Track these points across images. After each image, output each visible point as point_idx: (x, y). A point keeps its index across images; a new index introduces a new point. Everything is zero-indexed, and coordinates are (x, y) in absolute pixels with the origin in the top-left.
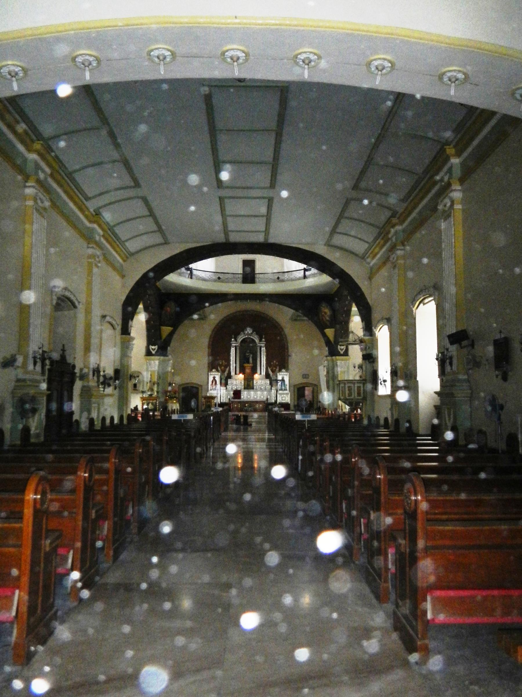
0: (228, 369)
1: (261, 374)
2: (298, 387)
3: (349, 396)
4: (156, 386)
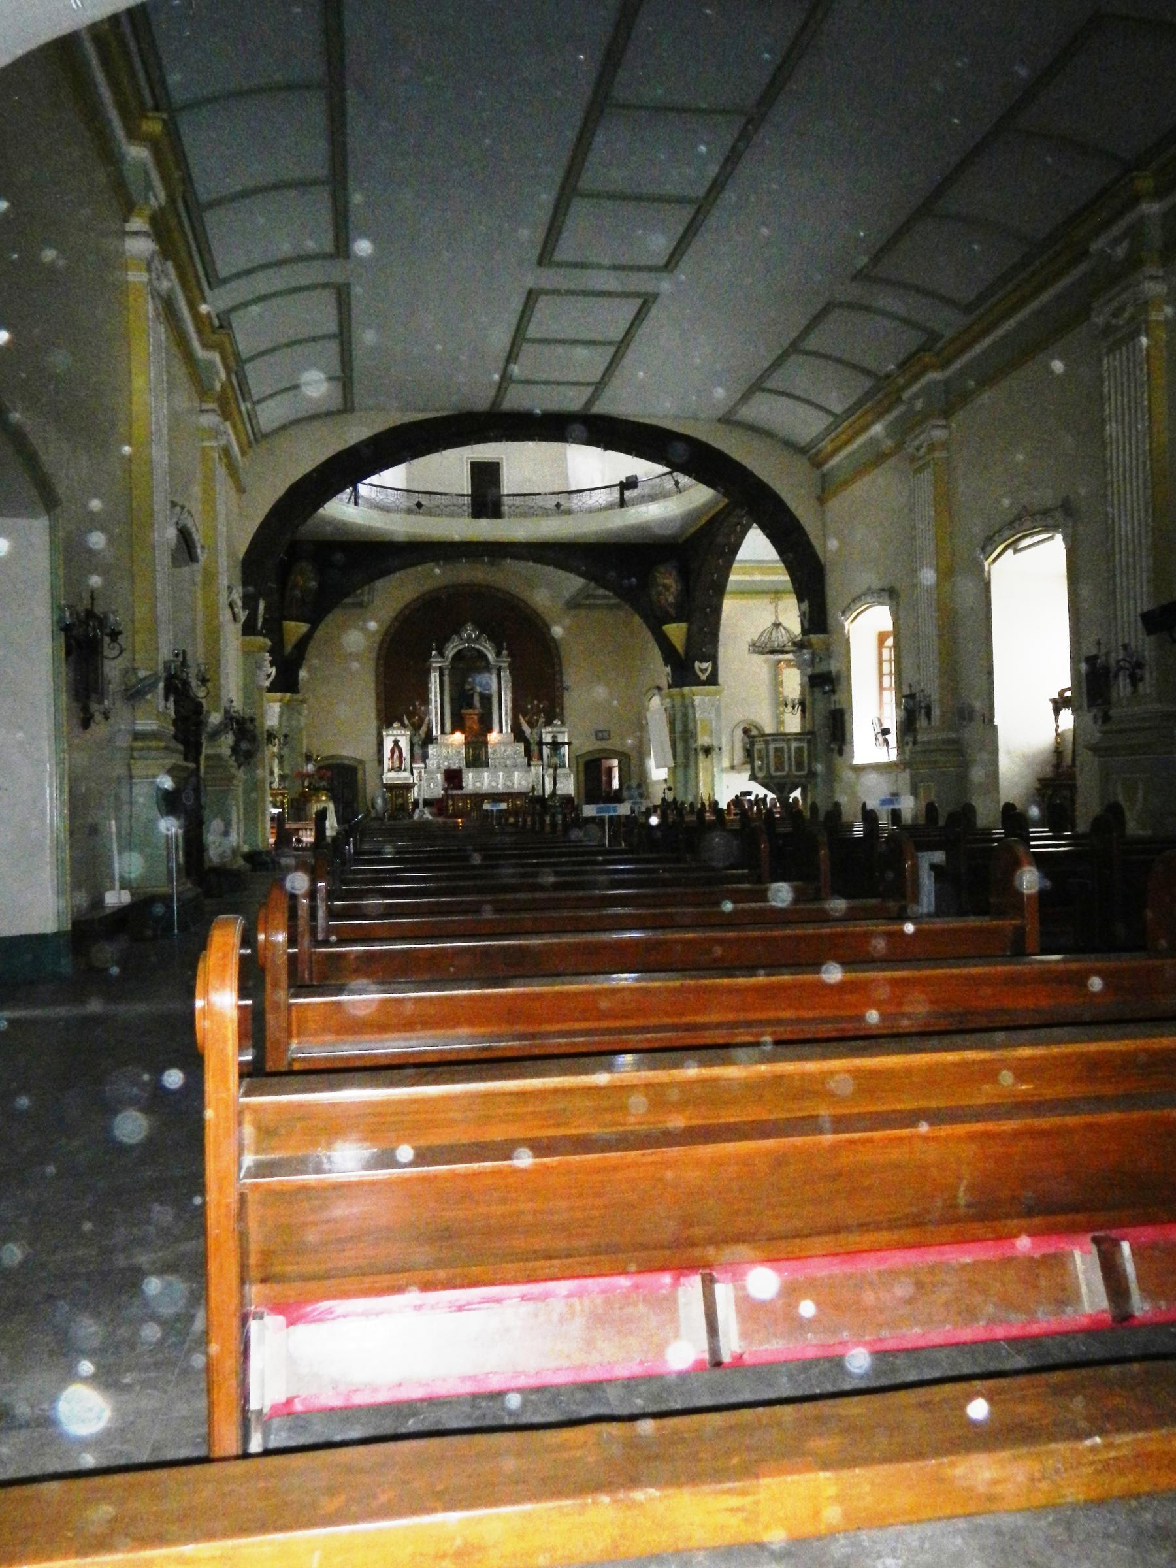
1: (501, 731)
2: (588, 758)
3: (777, 769)
4: (276, 761)
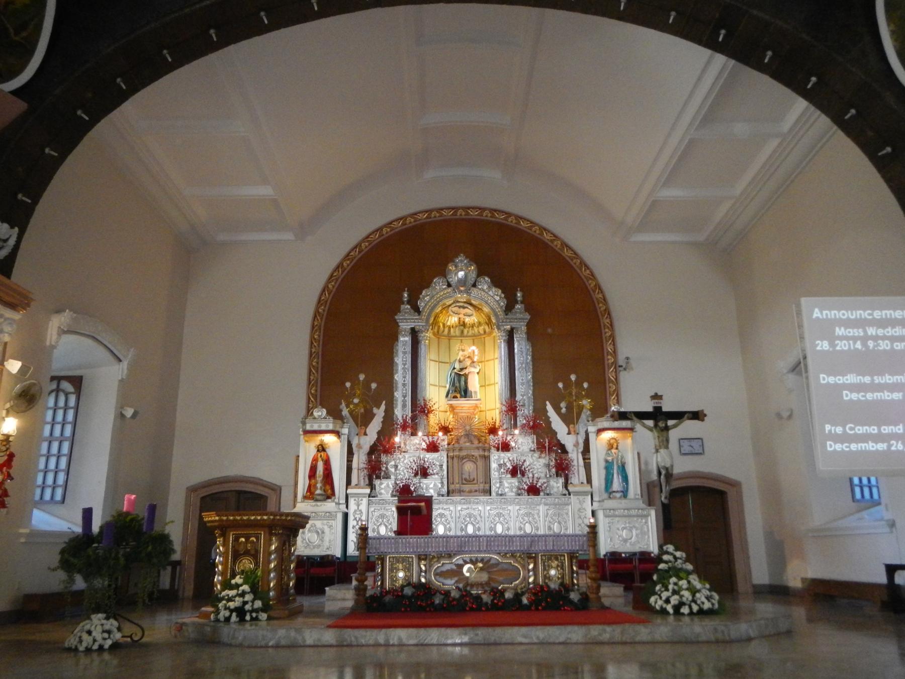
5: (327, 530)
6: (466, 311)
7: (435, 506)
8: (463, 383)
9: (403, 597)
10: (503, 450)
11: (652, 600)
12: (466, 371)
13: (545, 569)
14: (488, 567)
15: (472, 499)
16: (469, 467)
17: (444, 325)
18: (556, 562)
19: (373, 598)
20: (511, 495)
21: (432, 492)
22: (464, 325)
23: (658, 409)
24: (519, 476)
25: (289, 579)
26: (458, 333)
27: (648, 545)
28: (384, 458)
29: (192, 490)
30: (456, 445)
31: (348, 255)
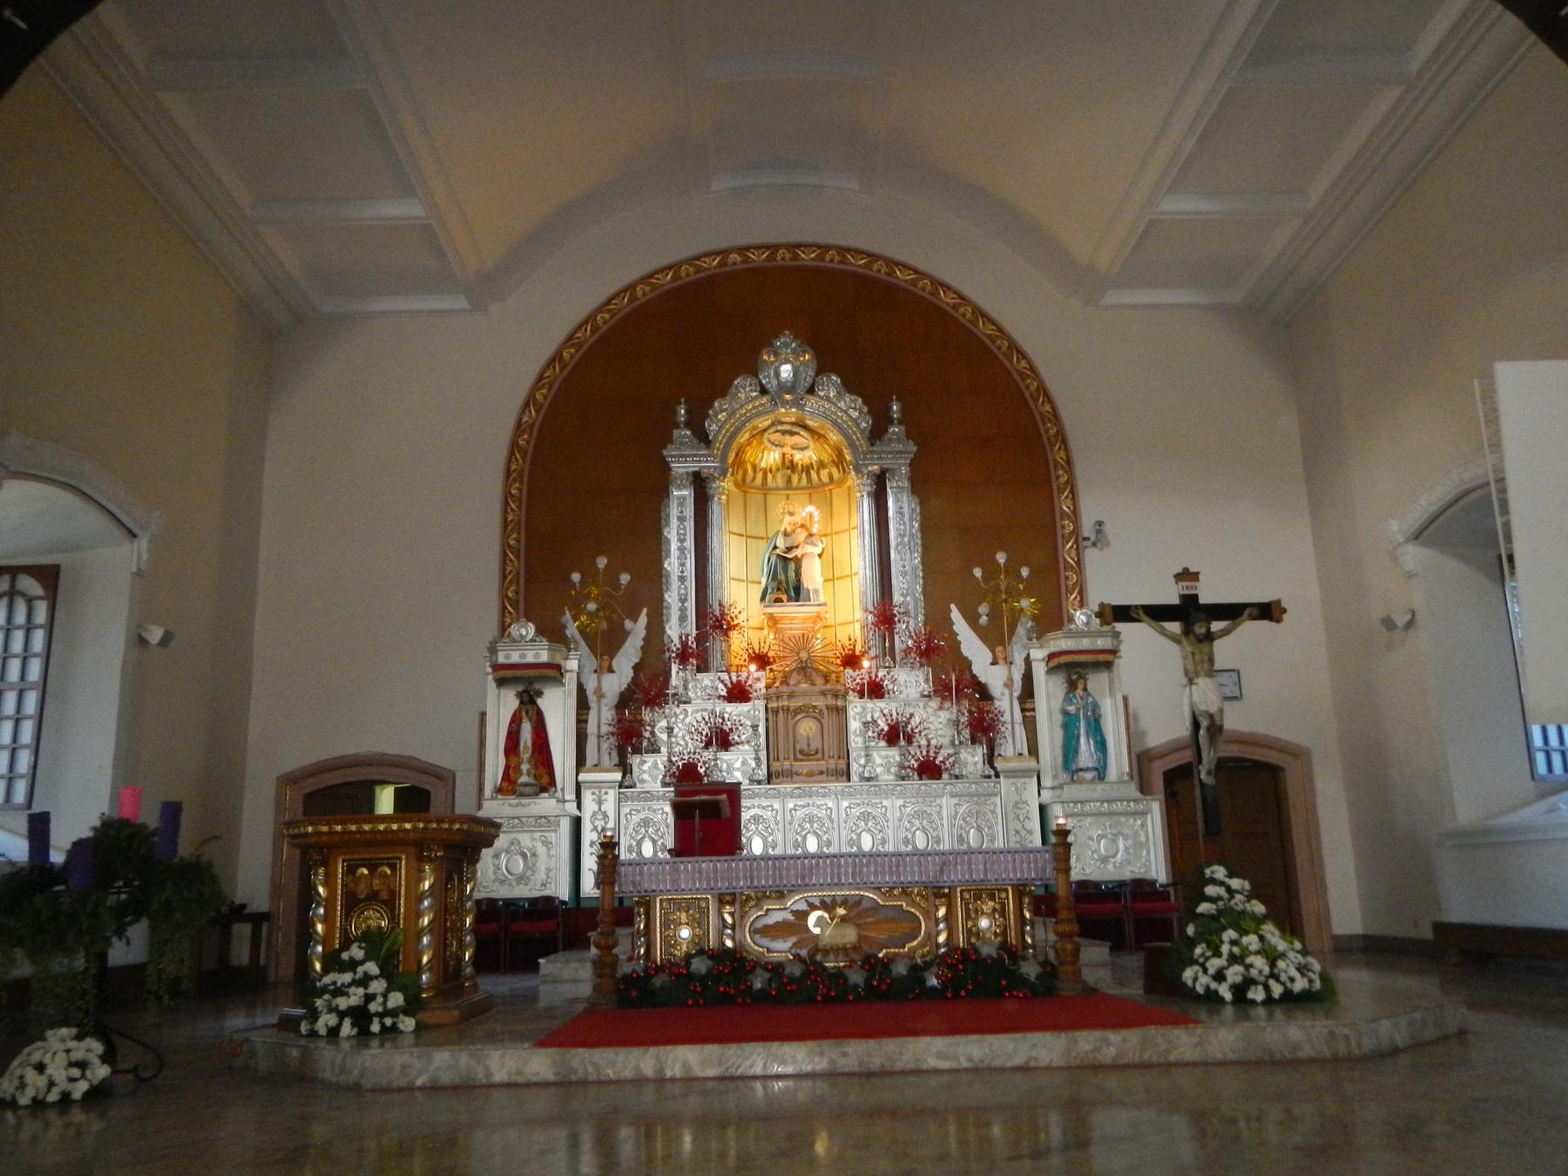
0: (638, 629)
5: (541, 849)
6: (796, 439)
7: (745, 803)
8: (792, 574)
9: (690, 977)
10: (870, 697)
11: (1188, 974)
12: (798, 553)
13: (968, 917)
14: (859, 915)
15: (815, 787)
16: (807, 728)
17: (754, 467)
18: (991, 904)
19: (630, 980)
20: (888, 778)
21: (738, 776)
22: (792, 466)
23: (1190, 600)
24: (902, 743)
25: (462, 947)
26: (780, 482)
27: (1148, 869)
28: (646, 715)
29: (289, 780)
30: (784, 688)
31: (571, 337)
